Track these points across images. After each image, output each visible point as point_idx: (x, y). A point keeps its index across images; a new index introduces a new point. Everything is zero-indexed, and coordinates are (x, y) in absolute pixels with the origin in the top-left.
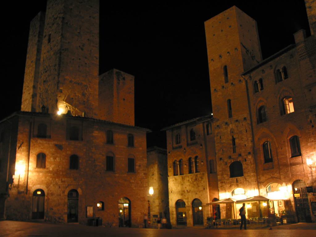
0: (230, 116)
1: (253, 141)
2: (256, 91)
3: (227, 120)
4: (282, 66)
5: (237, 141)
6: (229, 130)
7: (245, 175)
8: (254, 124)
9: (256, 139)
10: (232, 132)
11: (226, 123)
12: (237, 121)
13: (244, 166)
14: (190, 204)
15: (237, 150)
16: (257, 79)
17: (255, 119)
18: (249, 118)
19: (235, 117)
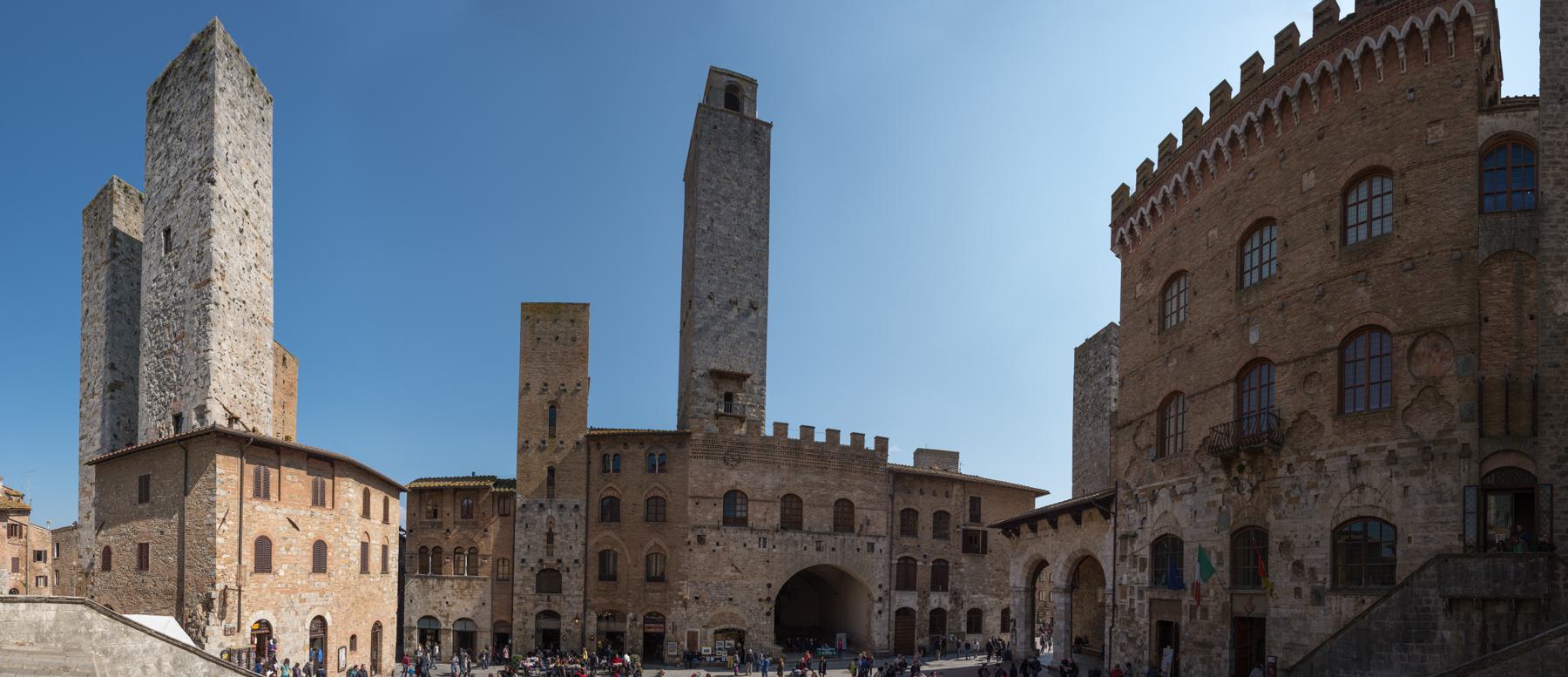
0: (551, 496)
1: (586, 545)
2: (605, 470)
3: (544, 501)
4: (661, 451)
5: (557, 538)
6: (545, 517)
7: (565, 593)
8: (591, 520)
9: (591, 543)
10: (551, 521)
11: (541, 505)
12: (561, 506)
13: (565, 578)
14: (450, 627)
15: (557, 555)
16: (612, 452)
17: (595, 511)
18: (583, 508)
19: (559, 500)
